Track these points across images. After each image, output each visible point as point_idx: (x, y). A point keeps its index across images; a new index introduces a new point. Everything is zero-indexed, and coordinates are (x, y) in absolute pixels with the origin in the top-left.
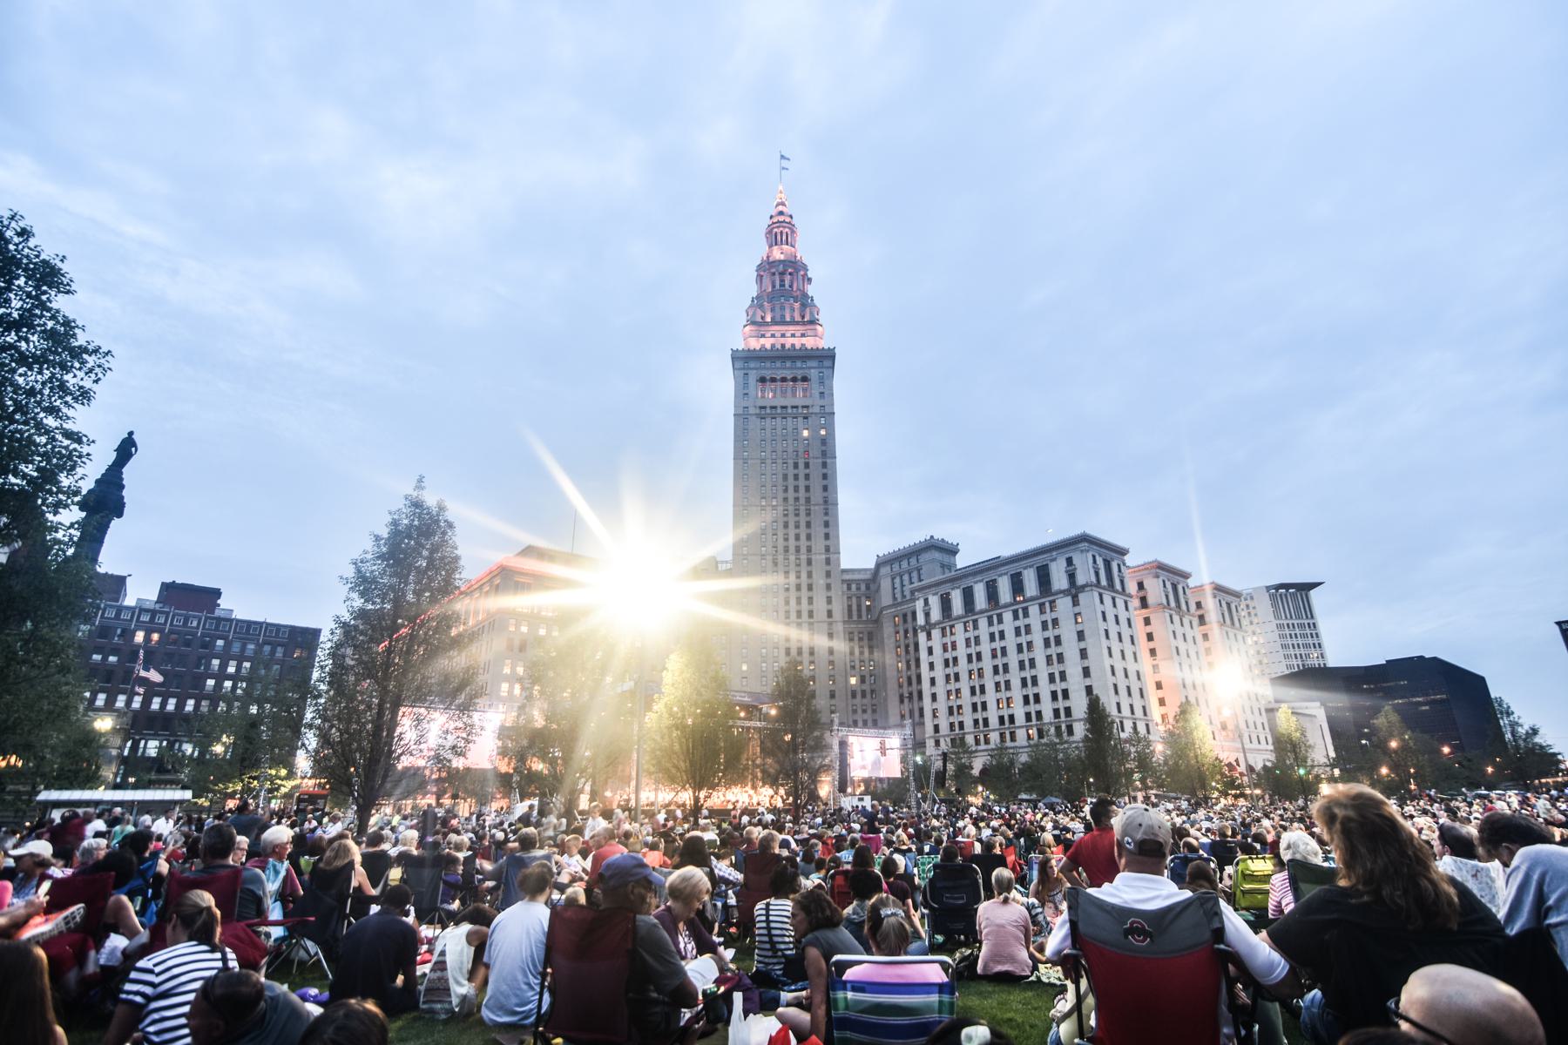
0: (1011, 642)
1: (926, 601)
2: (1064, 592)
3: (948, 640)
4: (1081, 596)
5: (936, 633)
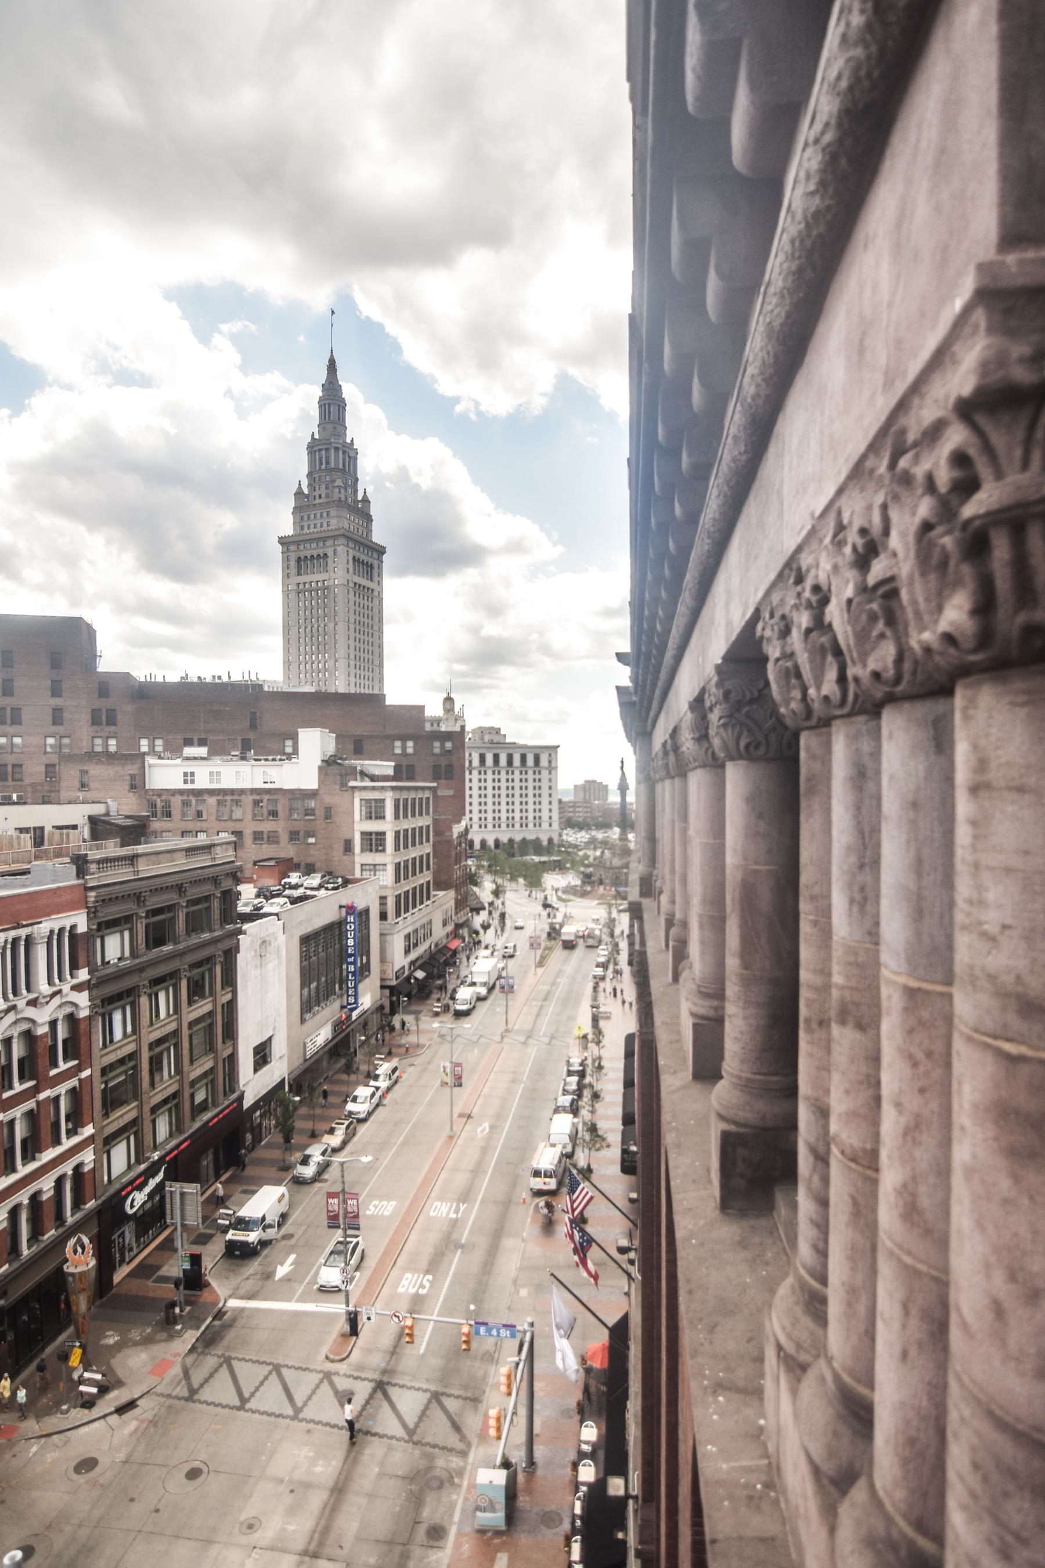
1: (470, 755)
2: (546, 768)
4: (553, 772)
5: (475, 773)
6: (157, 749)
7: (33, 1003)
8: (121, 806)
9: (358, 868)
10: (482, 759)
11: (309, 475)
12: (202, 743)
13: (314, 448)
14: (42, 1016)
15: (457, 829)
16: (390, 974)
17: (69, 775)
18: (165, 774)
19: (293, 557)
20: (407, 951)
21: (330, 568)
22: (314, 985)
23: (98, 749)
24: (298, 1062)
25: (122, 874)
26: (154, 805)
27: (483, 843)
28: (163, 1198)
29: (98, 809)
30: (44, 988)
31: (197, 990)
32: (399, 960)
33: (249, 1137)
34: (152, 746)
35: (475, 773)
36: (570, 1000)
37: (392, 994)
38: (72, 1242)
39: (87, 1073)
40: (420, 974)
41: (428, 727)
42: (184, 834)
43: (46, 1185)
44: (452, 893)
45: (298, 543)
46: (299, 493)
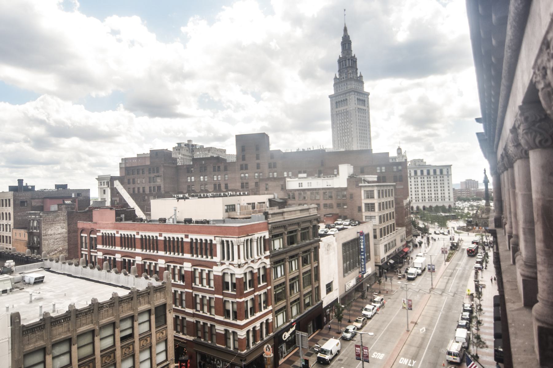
3: (416, 180)
5: (413, 178)
6: (290, 175)
7: (253, 261)
8: (277, 195)
9: (364, 217)
10: (416, 172)
11: (339, 71)
12: (304, 172)
13: (340, 61)
14: (256, 266)
15: (405, 202)
16: (379, 261)
17: (262, 186)
18: (293, 184)
20: (386, 251)
21: (348, 104)
22: (348, 263)
23: (271, 176)
24: (343, 292)
25: (278, 219)
26: (289, 195)
27: (418, 208)
28: (295, 336)
29: (271, 197)
30: (256, 257)
31: (305, 262)
32: (383, 255)
33: (325, 318)
34: (288, 174)
35: (413, 178)
37: (380, 269)
38: (266, 346)
39: (269, 288)
40: (392, 261)
41: (391, 161)
42: (299, 205)
43: (257, 324)
44: (404, 229)
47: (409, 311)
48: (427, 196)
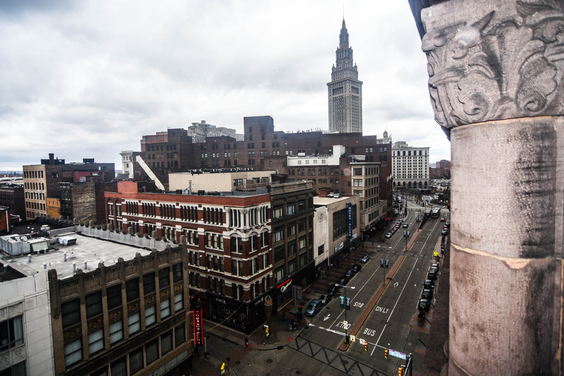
0: (412, 162)
5: (396, 158)
6: (291, 154)
7: (257, 228)
8: (279, 171)
9: (353, 191)
10: (399, 153)
11: (337, 61)
12: (303, 151)
13: (338, 52)
14: (259, 231)
15: (388, 179)
16: (363, 227)
17: (267, 162)
18: (293, 162)
19: (332, 89)
20: (370, 220)
21: (344, 91)
22: (337, 229)
23: (274, 154)
24: (332, 253)
25: (280, 192)
26: (290, 171)
27: (399, 183)
28: (291, 290)
29: (274, 172)
30: (259, 224)
31: (301, 229)
32: (367, 222)
33: (317, 275)
34: (289, 153)
36: (433, 242)
37: (364, 234)
38: (267, 297)
39: (270, 249)
40: (374, 228)
41: (378, 143)
42: (298, 180)
43: (260, 280)
44: (386, 201)
45: (333, 84)
46: (333, 68)
47: (386, 269)
48: (407, 174)
